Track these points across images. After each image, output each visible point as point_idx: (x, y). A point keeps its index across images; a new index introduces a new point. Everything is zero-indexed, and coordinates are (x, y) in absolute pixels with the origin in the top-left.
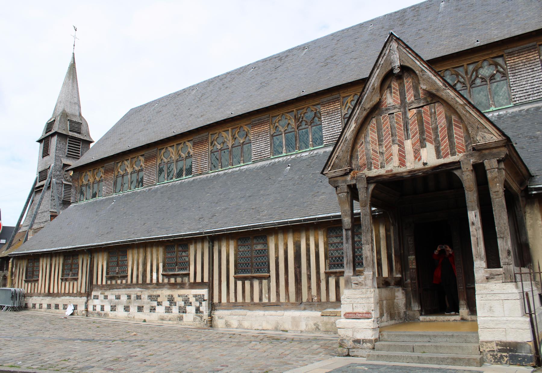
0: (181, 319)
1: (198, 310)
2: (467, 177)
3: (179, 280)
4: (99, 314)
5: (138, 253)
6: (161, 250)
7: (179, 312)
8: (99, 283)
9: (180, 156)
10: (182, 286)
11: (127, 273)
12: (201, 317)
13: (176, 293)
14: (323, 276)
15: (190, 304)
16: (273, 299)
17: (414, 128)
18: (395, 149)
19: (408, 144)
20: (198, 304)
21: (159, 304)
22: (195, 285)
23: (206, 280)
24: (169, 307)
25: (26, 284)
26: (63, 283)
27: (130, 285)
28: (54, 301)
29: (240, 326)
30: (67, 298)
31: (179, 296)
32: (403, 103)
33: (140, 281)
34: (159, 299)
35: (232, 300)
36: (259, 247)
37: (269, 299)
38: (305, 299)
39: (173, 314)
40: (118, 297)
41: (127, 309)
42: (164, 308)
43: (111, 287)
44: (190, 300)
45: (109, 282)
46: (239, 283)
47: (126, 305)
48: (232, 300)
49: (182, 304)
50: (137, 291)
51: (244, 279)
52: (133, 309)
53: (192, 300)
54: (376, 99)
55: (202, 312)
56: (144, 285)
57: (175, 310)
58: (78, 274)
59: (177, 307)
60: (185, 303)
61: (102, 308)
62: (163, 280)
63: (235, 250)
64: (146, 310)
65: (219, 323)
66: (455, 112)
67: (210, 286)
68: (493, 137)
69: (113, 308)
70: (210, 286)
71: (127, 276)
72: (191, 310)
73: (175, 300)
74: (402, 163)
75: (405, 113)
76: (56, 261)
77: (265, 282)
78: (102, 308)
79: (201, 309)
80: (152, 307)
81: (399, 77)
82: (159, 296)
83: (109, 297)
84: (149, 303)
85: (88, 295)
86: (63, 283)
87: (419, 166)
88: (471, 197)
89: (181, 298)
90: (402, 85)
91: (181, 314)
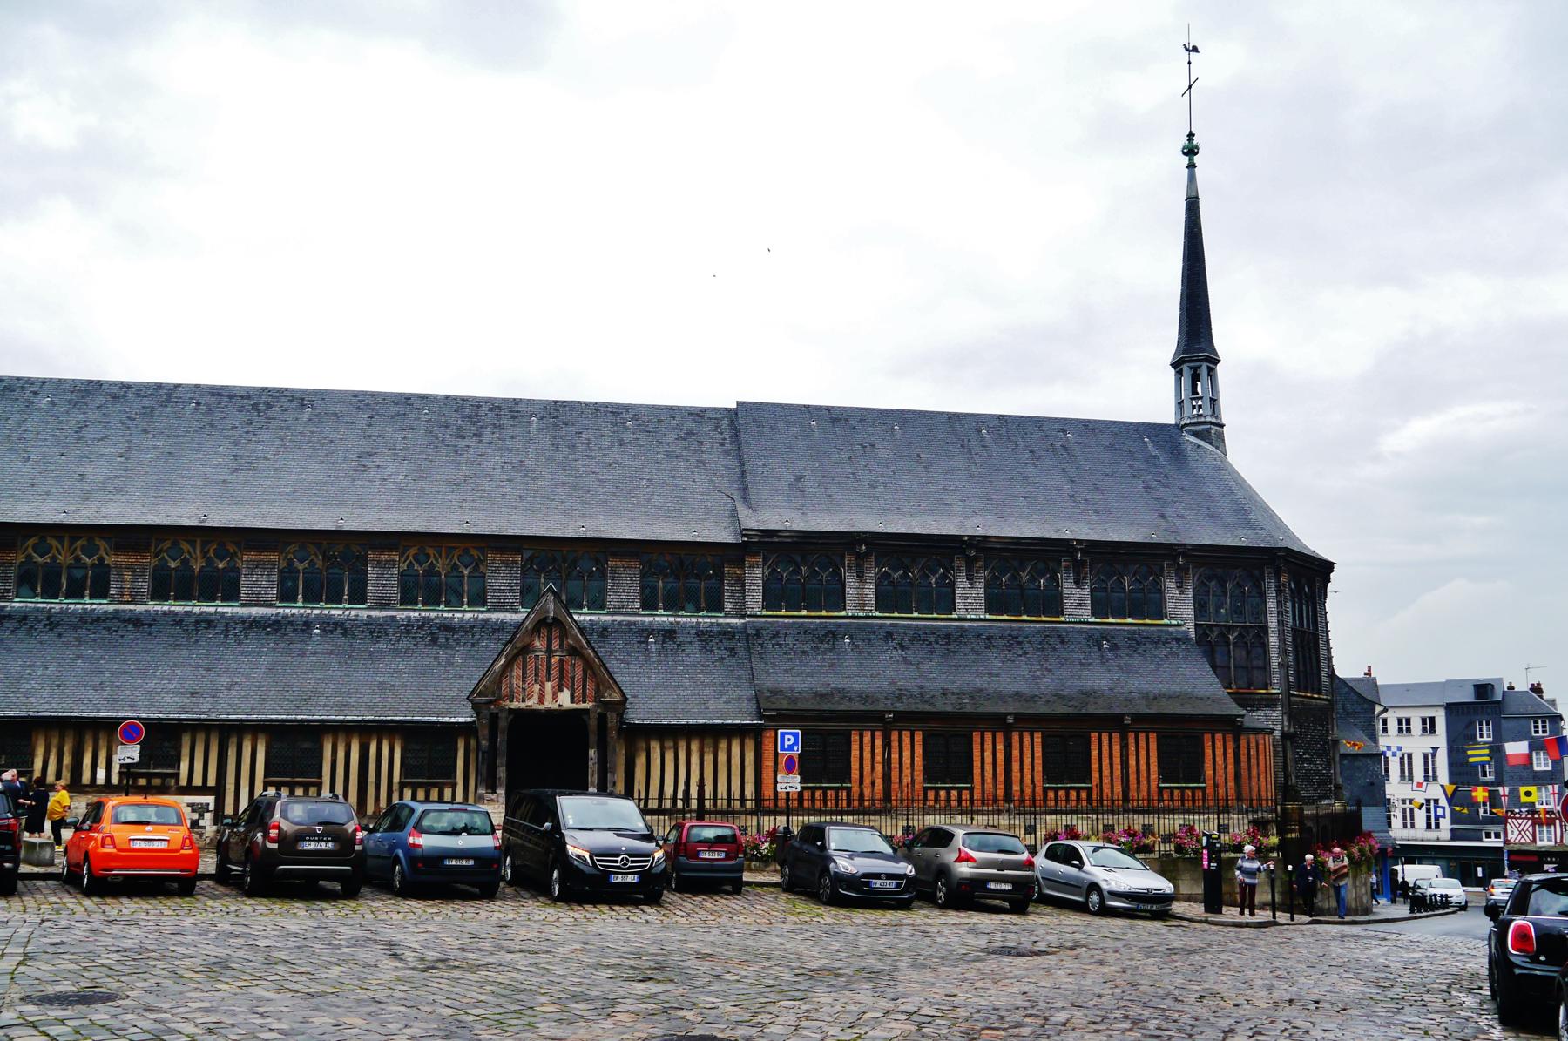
2: (593, 723)
9: (78, 559)
10: (163, 790)
14: (396, 787)
17: (555, 673)
18: (537, 687)
19: (549, 686)
20: (196, 816)
22: (189, 790)
23: (211, 782)
32: (549, 652)
36: (306, 745)
54: (527, 640)
66: (592, 668)
68: (617, 697)
70: (218, 792)
71: (32, 772)
74: (541, 702)
75: (549, 659)
81: (549, 626)
87: (555, 706)
88: (593, 738)
90: (550, 633)
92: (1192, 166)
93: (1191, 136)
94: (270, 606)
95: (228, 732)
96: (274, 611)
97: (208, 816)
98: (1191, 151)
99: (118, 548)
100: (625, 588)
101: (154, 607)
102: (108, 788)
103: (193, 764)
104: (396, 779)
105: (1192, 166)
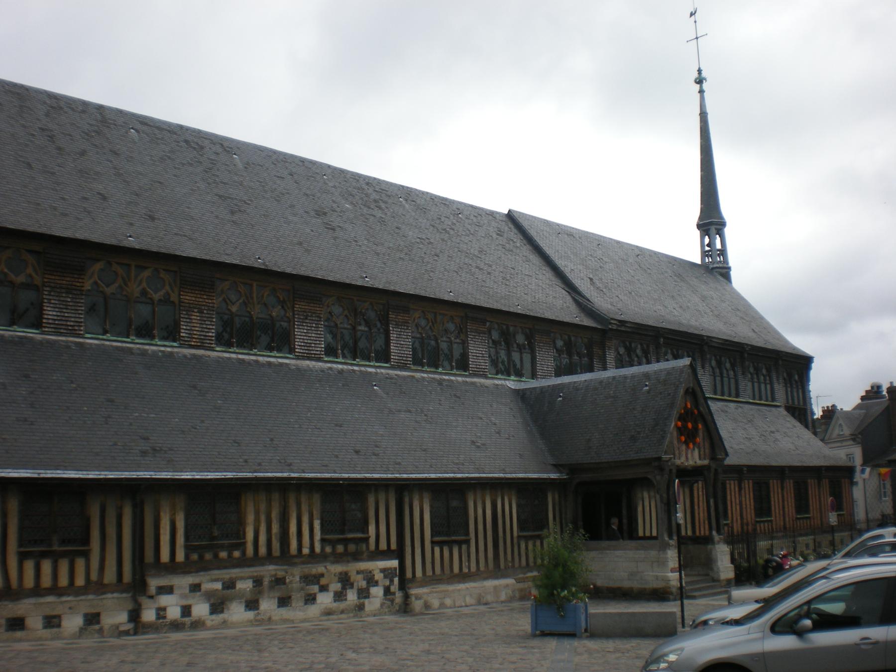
0: (361, 607)
1: (387, 591)
3: (352, 547)
4: (176, 626)
5: (269, 502)
6: (317, 498)
7: (359, 598)
8: (165, 556)
10: (356, 557)
11: (244, 538)
12: (392, 601)
13: (353, 568)
14: (515, 540)
15: (376, 584)
20: (387, 583)
21: (324, 589)
22: (379, 554)
23: (394, 546)
24: (341, 593)
26: (29, 565)
29: (442, 605)
30: (50, 599)
31: (358, 572)
34: (323, 581)
35: (429, 572)
36: (455, 504)
38: (502, 566)
39: (348, 603)
40: (230, 585)
41: (252, 605)
42: (331, 594)
43: (202, 566)
44: (376, 578)
45: (195, 557)
46: (437, 550)
48: (429, 572)
49: (364, 584)
50: (269, 570)
51: (441, 544)
52: (268, 605)
53: (379, 576)
55: (394, 594)
56: (285, 557)
57: (352, 596)
58: (86, 541)
59: (355, 591)
60: (368, 583)
61: (186, 611)
62: (323, 549)
63: (431, 507)
64: (297, 601)
65: (417, 605)
67: (399, 554)
69: (217, 607)
70: (399, 554)
71: (244, 543)
72: (377, 592)
73: (352, 580)
78: (186, 611)
79: (393, 589)
80: (310, 595)
82: (322, 575)
83: (206, 586)
84: (302, 589)
86: (29, 565)
89: (360, 577)
91: (362, 601)
92: (701, 92)
93: (700, 71)
94: (319, 359)
95: (402, 489)
96: (320, 364)
97: (396, 580)
98: (700, 81)
100: (546, 359)
101: (219, 353)
103: (379, 530)
104: (515, 534)
105: (701, 92)
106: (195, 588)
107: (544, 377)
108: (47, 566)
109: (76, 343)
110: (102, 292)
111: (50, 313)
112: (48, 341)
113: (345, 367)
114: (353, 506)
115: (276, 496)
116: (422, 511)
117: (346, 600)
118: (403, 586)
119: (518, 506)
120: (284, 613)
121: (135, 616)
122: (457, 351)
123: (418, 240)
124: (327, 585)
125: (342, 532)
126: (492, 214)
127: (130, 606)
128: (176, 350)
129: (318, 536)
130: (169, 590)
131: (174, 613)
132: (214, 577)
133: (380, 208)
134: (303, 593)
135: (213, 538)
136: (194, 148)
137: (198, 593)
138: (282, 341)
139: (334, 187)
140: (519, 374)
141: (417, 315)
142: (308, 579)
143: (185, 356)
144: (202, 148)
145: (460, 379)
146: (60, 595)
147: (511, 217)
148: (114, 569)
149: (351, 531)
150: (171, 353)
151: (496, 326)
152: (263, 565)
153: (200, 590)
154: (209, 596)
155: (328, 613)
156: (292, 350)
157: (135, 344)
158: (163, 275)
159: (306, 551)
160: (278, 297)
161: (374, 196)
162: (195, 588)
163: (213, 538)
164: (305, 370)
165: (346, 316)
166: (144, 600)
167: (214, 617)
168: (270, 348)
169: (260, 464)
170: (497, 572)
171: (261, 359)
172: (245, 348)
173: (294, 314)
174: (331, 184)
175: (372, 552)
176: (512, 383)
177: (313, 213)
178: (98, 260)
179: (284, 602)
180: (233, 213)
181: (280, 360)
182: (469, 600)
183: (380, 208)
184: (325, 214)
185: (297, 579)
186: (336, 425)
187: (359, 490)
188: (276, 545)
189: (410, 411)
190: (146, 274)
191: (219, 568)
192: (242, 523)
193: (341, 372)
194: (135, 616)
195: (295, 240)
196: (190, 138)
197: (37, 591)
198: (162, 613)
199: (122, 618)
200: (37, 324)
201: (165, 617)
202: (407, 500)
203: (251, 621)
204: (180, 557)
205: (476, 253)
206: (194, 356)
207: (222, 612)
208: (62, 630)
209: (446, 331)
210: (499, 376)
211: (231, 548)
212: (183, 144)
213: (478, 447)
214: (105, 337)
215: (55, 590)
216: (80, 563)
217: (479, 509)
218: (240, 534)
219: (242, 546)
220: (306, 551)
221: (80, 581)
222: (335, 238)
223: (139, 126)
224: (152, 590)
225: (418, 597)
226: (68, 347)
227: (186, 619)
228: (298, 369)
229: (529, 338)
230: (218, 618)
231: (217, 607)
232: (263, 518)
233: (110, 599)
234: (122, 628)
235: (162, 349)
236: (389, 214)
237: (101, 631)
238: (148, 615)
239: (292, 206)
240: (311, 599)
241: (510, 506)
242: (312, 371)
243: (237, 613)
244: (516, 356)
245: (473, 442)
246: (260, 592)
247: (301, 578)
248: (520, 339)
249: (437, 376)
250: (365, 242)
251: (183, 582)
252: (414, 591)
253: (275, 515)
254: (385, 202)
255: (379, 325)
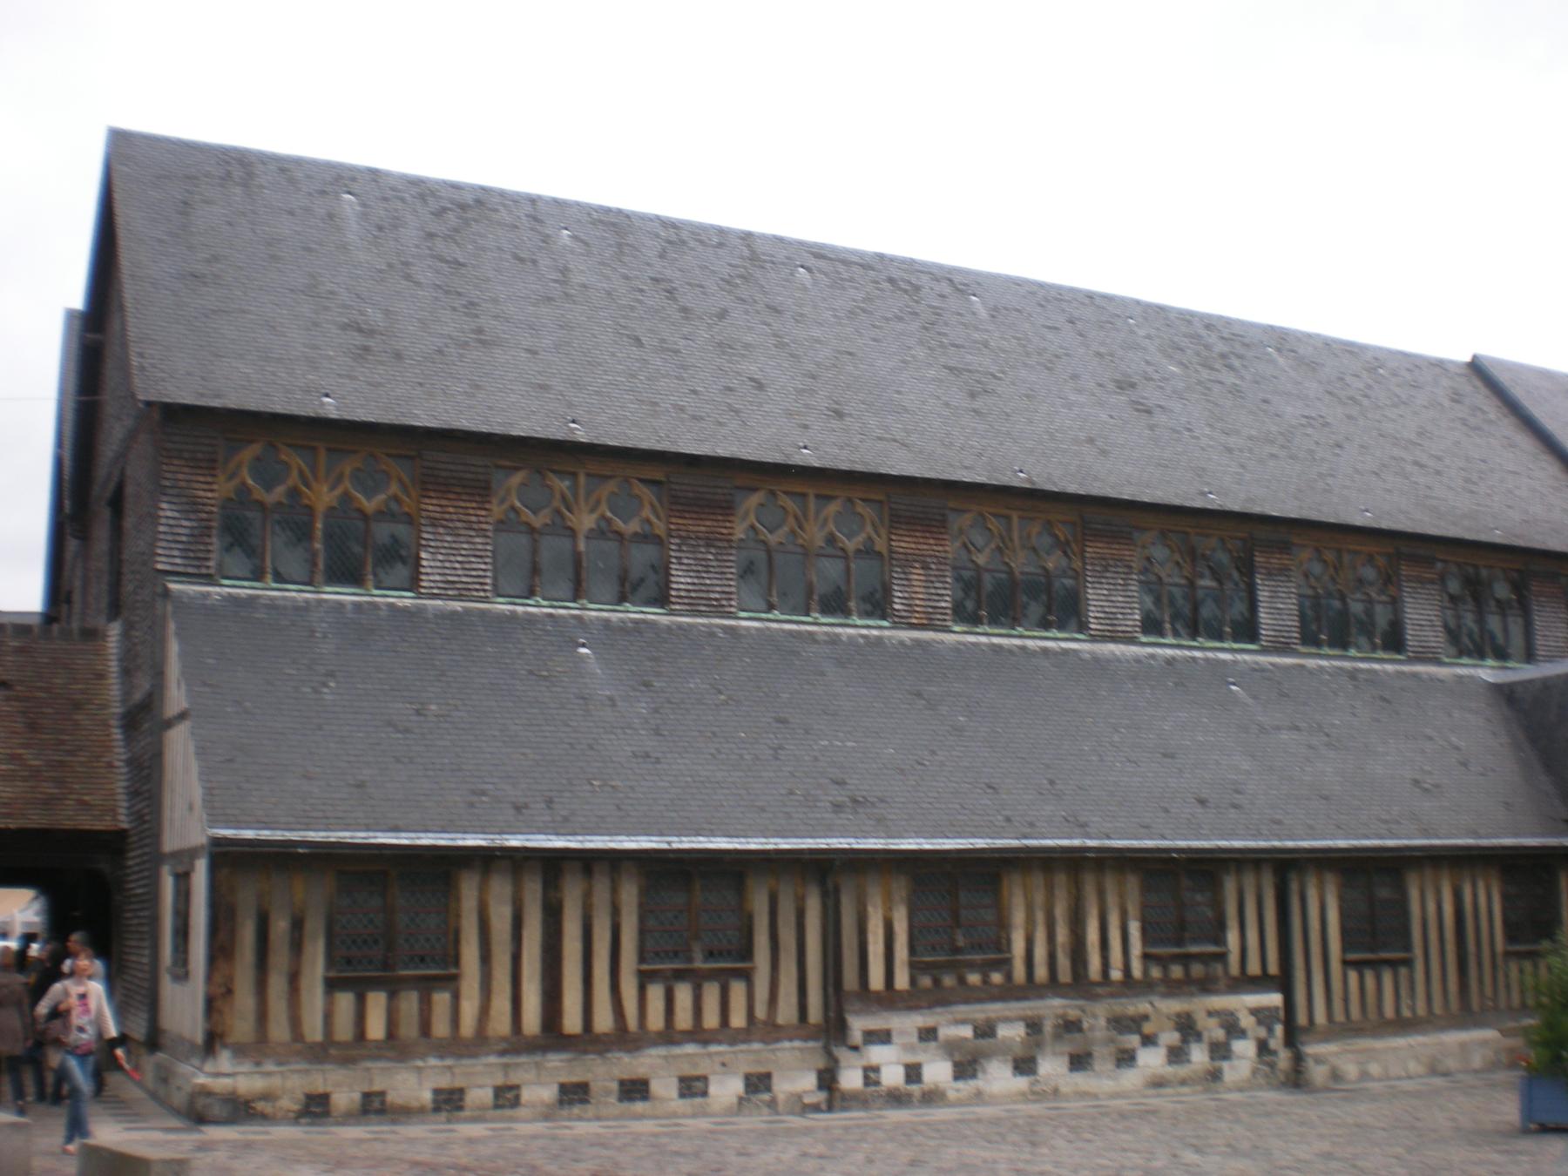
0: (1215, 1076)
1: (1263, 1048)
3: (1197, 970)
4: (896, 1098)
6: (1133, 883)
7: (1212, 1058)
10: (1206, 986)
11: (1009, 950)
12: (1272, 1066)
14: (1499, 960)
15: (1242, 1034)
16: (1421, 1010)
21: (1149, 1041)
23: (1273, 969)
24: (1180, 1049)
25: (345, 1001)
26: (656, 993)
27: (1020, 988)
28: (604, 1072)
29: (1365, 1075)
30: (690, 1048)
31: (1210, 1014)
33: (1065, 975)
34: (1148, 1028)
35: (1339, 1016)
37: (1413, 1009)
39: (1192, 1067)
40: (985, 1030)
41: (1024, 1065)
43: (937, 998)
45: (926, 981)
47: (1019, 1051)
48: (1339, 1016)
49: (1219, 1034)
50: (1052, 1007)
51: (1359, 965)
52: (1051, 1067)
53: (1247, 1021)
56: (1080, 985)
57: (1199, 1056)
58: (747, 953)
61: (913, 1073)
62: (1146, 972)
63: (1342, 899)
65: (1318, 1073)
67: (1284, 983)
69: (966, 1068)
70: (1284, 983)
72: (1245, 1048)
76: (587, 897)
77: (1403, 971)
78: (913, 1073)
83: (946, 1032)
85: (834, 1031)
86: (656, 993)
91: (1217, 1064)
94: (1131, 641)
95: (1286, 867)
97: (1279, 1029)
99: (897, 521)
101: (957, 636)
102: (1129, 985)
103: (1246, 938)
106: (928, 1034)
107: (1550, 659)
108: (683, 994)
109: (725, 629)
110: (764, 542)
111: (681, 580)
112: (680, 626)
113: (1178, 652)
114: (1199, 897)
115: (1061, 879)
116: (1323, 907)
117: (1189, 1061)
118: (1291, 1040)
119: (1505, 897)
120: (1081, 1080)
121: (828, 1080)
122: (1382, 617)
123: (1304, 421)
124: (1155, 1035)
125: (1179, 942)
126: (1439, 365)
127: (821, 1063)
128: (887, 633)
129: (1136, 948)
130: (884, 1037)
131: (892, 1076)
132: (959, 1016)
133: (1230, 367)
134: (1112, 1049)
135: (957, 950)
136: (906, 291)
137: (933, 1044)
138: (1065, 611)
139: (1149, 337)
140: (1501, 654)
141: (1305, 555)
142: (1121, 1024)
143: (902, 643)
144: (917, 288)
145: (1389, 667)
146: (705, 1042)
147: (1478, 369)
148: (794, 1000)
149: (1196, 940)
150: (879, 638)
151: (1454, 569)
152: (1041, 997)
153: (935, 1038)
154: (951, 1048)
155: (1158, 1083)
156: (1083, 627)
157: (820, 625)
158: (861, 507)
159: (1116, 975)
160: (1056, 536)
161: (1221, 347)
162: (928, 1034)
163: (957, 950)
164: (1108, 661)
165: (1178, 563)
166: (842, 1053)
167: (960, 1085)
168: (1045, 625)
169: (1032, 825)
170: (1466, 1016)
171: (1030, 643)
172: (1002, 625)
173: (1085, 564)
174: (1142, 332)
175: (1235, 979)
176: (1488, 672)
177: (1111, 386)
178: (755, 490)
179: (1079, 1062)
180: (973, 395)
181: (1064, 645)
182: (1413, 1067)
183: (1230, 367)
184: (1133, 385)
185: (1102, 1022)
186: (1165, 755)
187: (1208, 868)
188: (1064, 963)
189: (1297, 728)
190: (833, 508)
191: (967, 1001)
192: (1003, 925)
193: (1170, 662)
194: (828, 1080)
195: (1082, 435)
196: (895, 274)
197: (669, 1036)
198: (872, 1075)
199: (805, 1082)
200: (661, 599)
201: (877, 1083)
202: (1294, 887)
203: (1023, 1094)
204: (902, 981)
205: (1413, 437)
206: (918, 643)
207: (974, 1076)
208: (709, 1100)
209: (1361, 582)
210: (1465, 660)
211: (986, 968)
212: (886, 285)
213: (1426, 790)
214: (770, 616)
215: (698, 1034)
216: (738, 990)
217: (1429, 904)
218: (1001, 944)
219: (1004, 964)
220: (1116, 975)
221: (738, 1020)
222: (1152, 428)
223: (811, 262)
224: (856, 1036)
225: (1319, 1060)
226: (712, 635)
227: (914, 1088)
228: (1096, 659)
229: (1519, 587)
230: (966, 1087)
231: (966, 1068)
232: (1040, 917)
233: (788, 1050)
234: (807, 1100)
235: (864, 632)
236: (1248, 377)
237: (772, 1104)
238: (851, 1079)
239: (1075, 377)
240: (1126, 1058)
241: (1487, 899)
242: (1119, 660)
243: (999, 1078)
244: (1494, 623)
245: (1416, 782)
246: (1039, 1045)
247: (1109, 1021)
248: (1502, 591)
249: (1347, 664)
250: (1207, 431)
251: (906, 1024)
252: (1311, 1049)
253: (1060, 911)
254: (1240, 357)
255: (1236, 575)
